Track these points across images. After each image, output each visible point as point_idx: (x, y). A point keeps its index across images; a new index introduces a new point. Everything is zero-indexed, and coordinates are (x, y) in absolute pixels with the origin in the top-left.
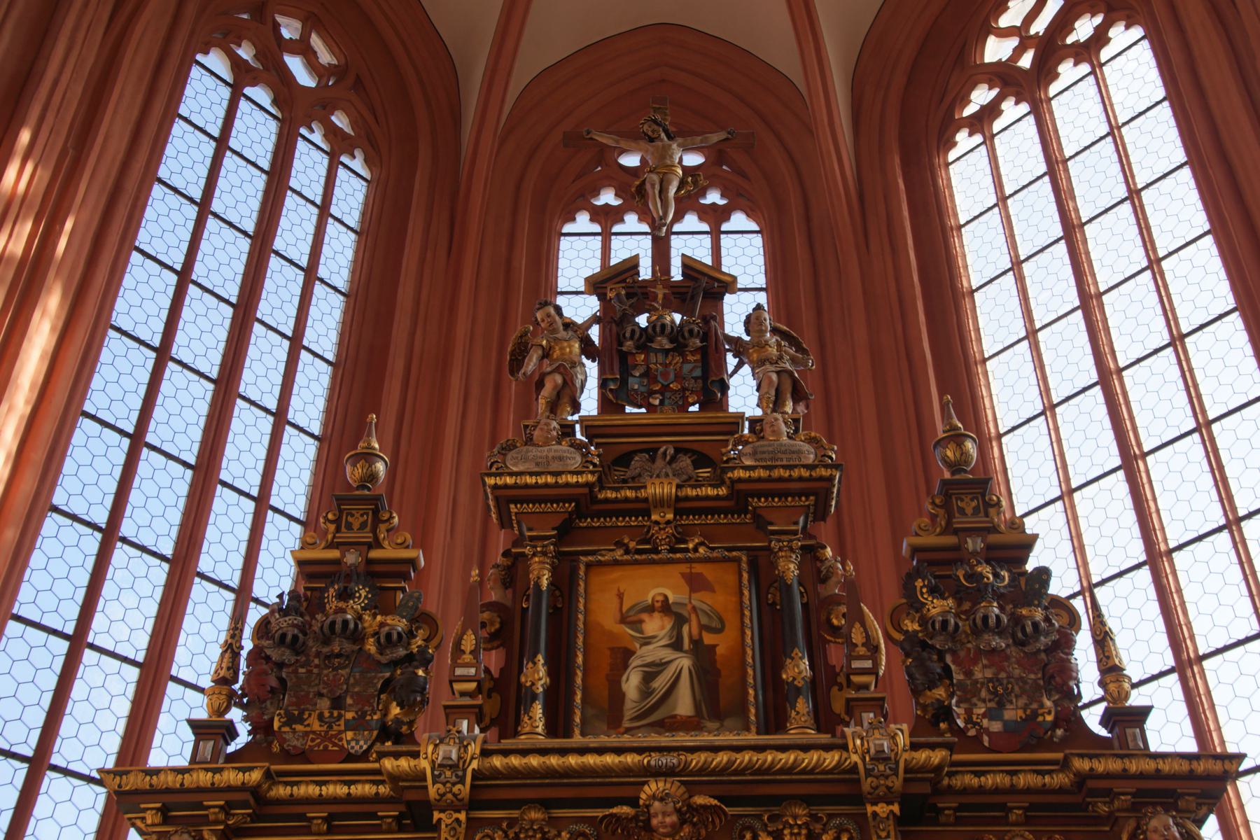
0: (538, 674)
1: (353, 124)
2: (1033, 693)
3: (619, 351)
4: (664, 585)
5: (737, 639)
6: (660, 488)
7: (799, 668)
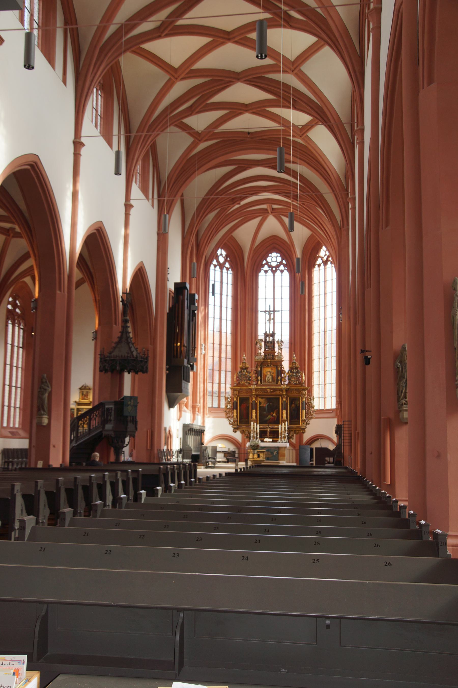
0: (259, 378)
1: (230, 264)
2: (297, 381)
3: (266, 342)
4: (269, 369)
5: (275, 375)
6: (269, 361)
7: (279, 378)
